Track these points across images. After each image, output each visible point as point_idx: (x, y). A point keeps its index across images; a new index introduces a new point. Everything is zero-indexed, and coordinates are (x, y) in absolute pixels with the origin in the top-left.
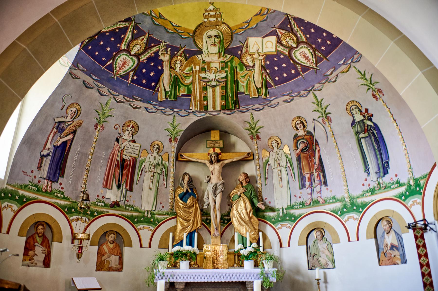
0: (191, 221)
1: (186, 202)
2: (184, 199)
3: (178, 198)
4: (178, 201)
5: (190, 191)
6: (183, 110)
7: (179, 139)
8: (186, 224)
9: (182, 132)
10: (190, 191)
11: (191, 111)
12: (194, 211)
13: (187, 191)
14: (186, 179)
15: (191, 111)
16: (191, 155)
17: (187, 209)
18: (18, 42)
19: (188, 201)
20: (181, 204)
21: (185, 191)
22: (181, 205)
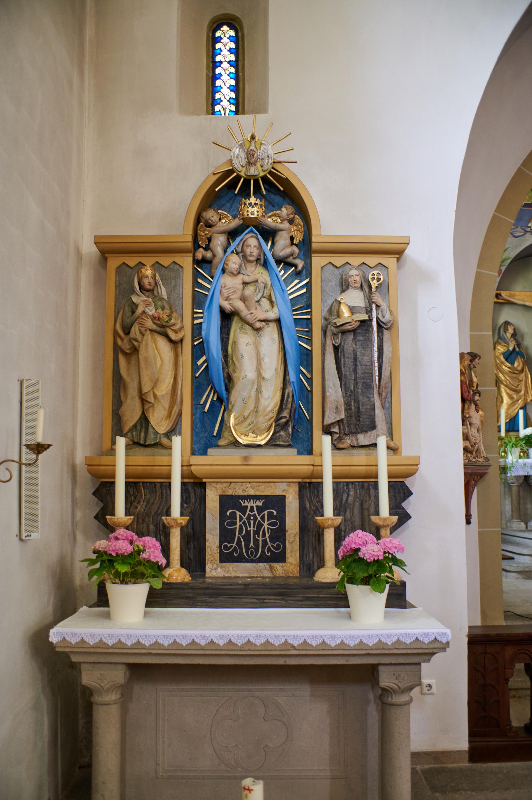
0: (523, 392)
1: (512, 363)
2: (509, 359)
3: (503, 359)
4: (502, 363)
5: (517, 349)
6: (519, 227)
7: (503, 271)
8: (515, 396)
9: (509, 261)
10: (517, 349)
11: (529, 229)
12: (524, 378)
13: (514, 349)
14: (511, 330)
15: (529, 229)
16: (511, 294)
17: (515, 375)
18: (523, 168)
19: (516, 364)
20: (506, 367)
21: (511, 348)
22: (507, 368)
